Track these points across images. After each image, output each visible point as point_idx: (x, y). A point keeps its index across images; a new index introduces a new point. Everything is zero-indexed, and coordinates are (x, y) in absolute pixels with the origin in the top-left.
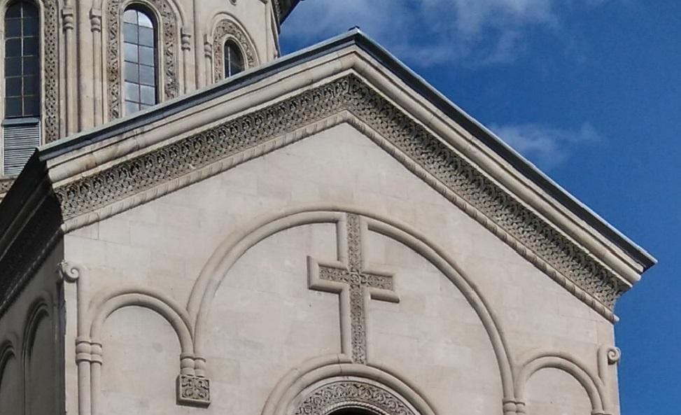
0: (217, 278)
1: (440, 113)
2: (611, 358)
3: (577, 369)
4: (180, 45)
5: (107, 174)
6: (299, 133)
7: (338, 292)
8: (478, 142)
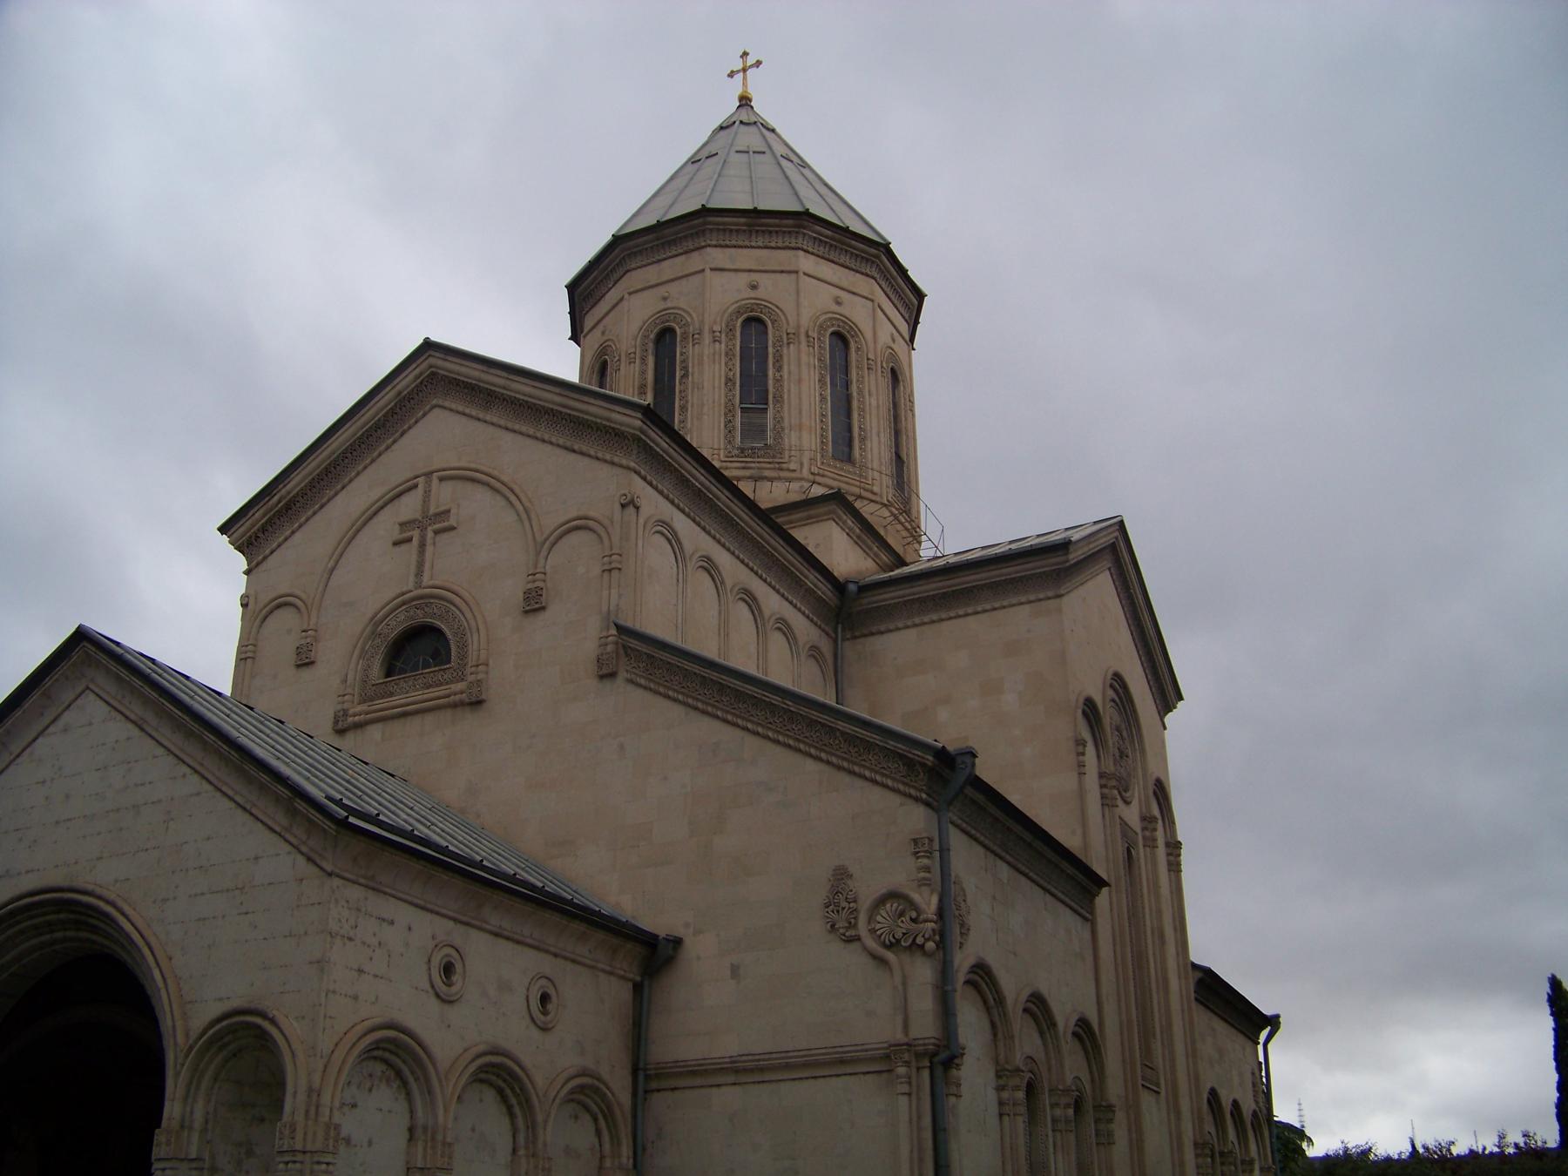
0: (332, 563)
1: (485, 368)
2: (622, 502)
3: (591, 523)
4: (691, 344)
5: (270, 521)
6: (397, 434)
7: (410, 540)
8: (511, 377)
